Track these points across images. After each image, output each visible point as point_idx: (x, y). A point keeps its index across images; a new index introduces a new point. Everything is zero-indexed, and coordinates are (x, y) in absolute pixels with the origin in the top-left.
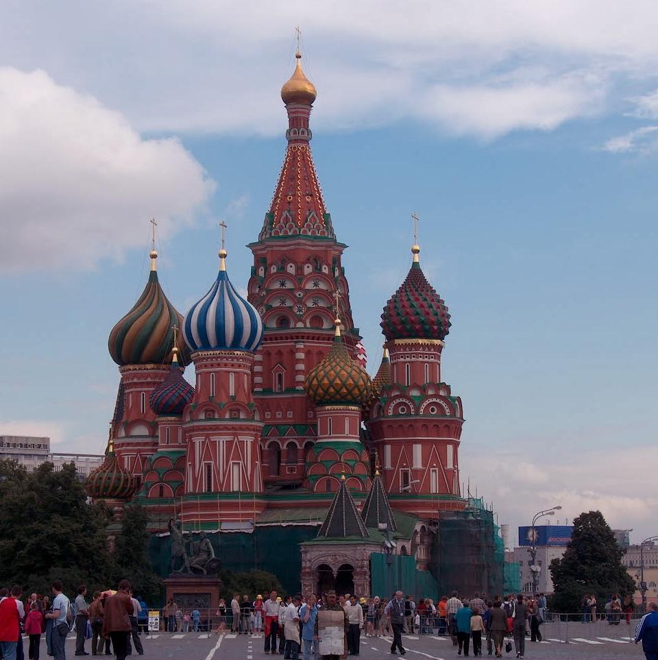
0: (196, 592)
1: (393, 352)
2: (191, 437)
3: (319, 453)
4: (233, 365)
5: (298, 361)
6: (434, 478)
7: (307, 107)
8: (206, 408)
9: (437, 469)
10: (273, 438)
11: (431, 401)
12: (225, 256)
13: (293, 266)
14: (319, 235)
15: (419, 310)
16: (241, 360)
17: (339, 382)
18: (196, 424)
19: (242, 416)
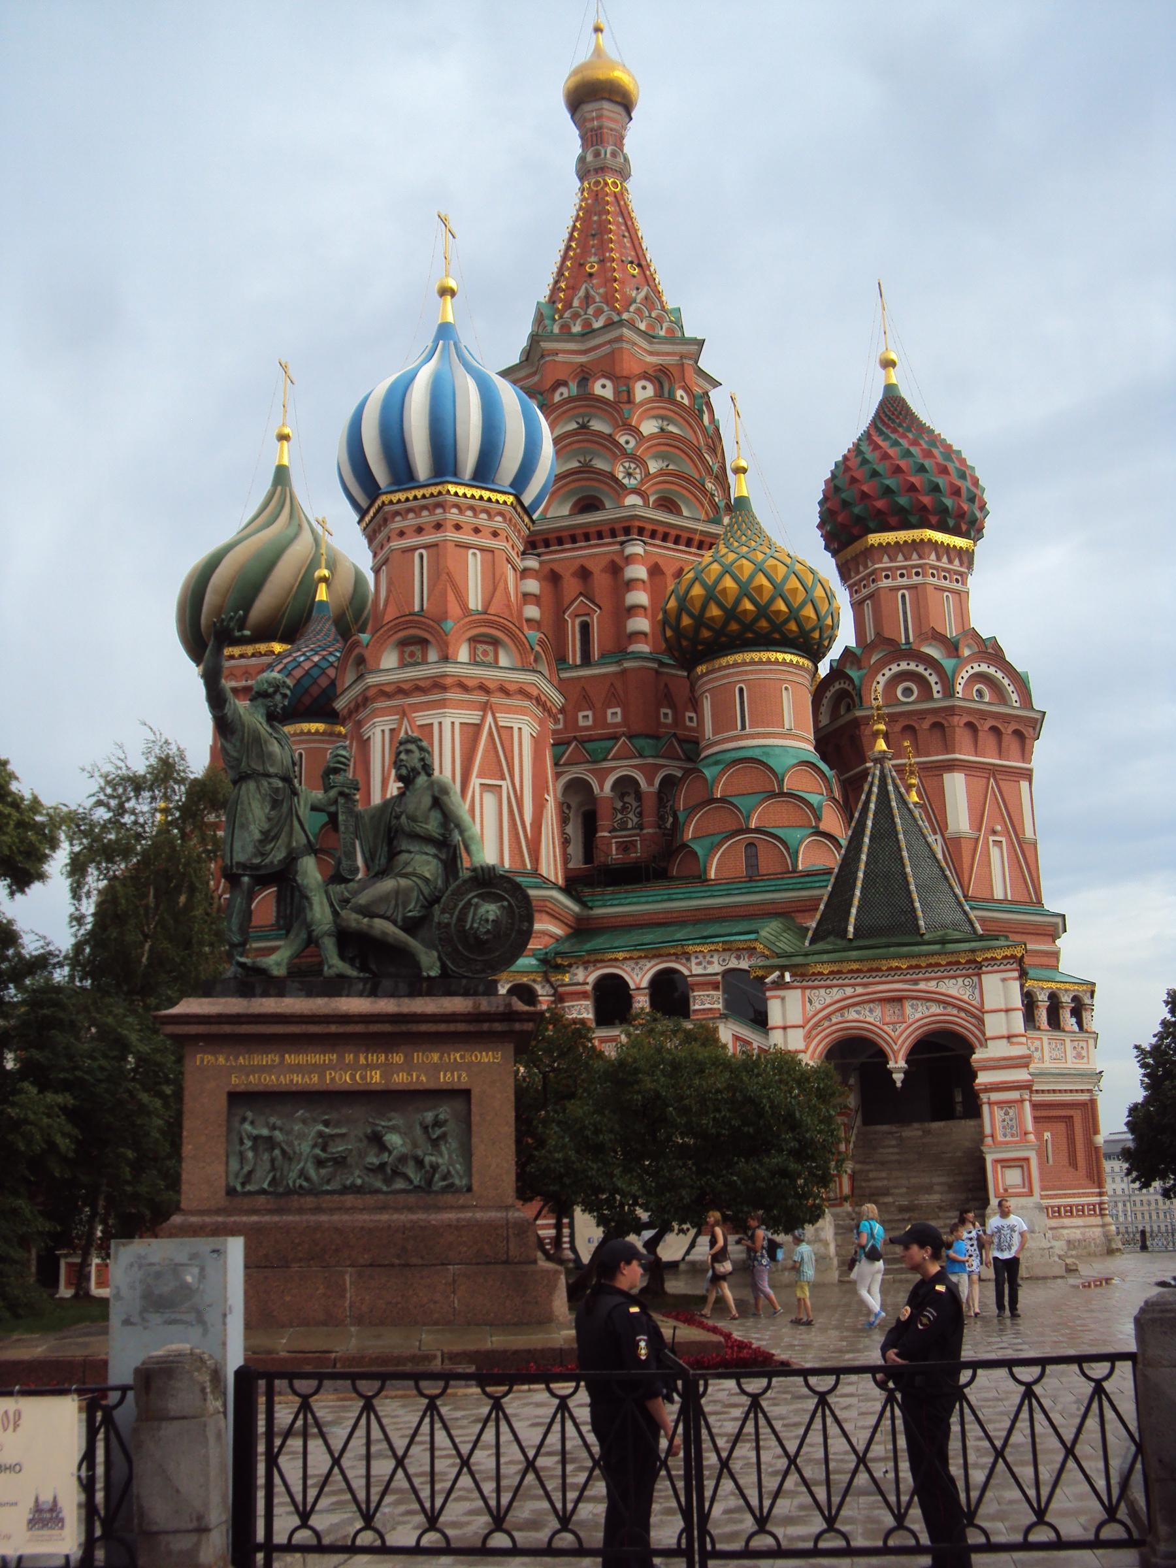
0: (375, 1078)
1: (858, 573)
2: (359, 724)
3: (716, 780)
4: (477, 530)
5: (630, 584)
6: (998, 860)
7: (624, 113)
8: (401, 634)
9: (1003, 839)
10: (574, 769)
11: (977, 669)
12: (453, 293)
13: (609, 384)
14: (662, 333)
15: (927, 463)
16: (499, 519)
17: (765, 582)
18: (372, 680)
19: (504, 661)
